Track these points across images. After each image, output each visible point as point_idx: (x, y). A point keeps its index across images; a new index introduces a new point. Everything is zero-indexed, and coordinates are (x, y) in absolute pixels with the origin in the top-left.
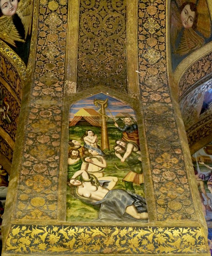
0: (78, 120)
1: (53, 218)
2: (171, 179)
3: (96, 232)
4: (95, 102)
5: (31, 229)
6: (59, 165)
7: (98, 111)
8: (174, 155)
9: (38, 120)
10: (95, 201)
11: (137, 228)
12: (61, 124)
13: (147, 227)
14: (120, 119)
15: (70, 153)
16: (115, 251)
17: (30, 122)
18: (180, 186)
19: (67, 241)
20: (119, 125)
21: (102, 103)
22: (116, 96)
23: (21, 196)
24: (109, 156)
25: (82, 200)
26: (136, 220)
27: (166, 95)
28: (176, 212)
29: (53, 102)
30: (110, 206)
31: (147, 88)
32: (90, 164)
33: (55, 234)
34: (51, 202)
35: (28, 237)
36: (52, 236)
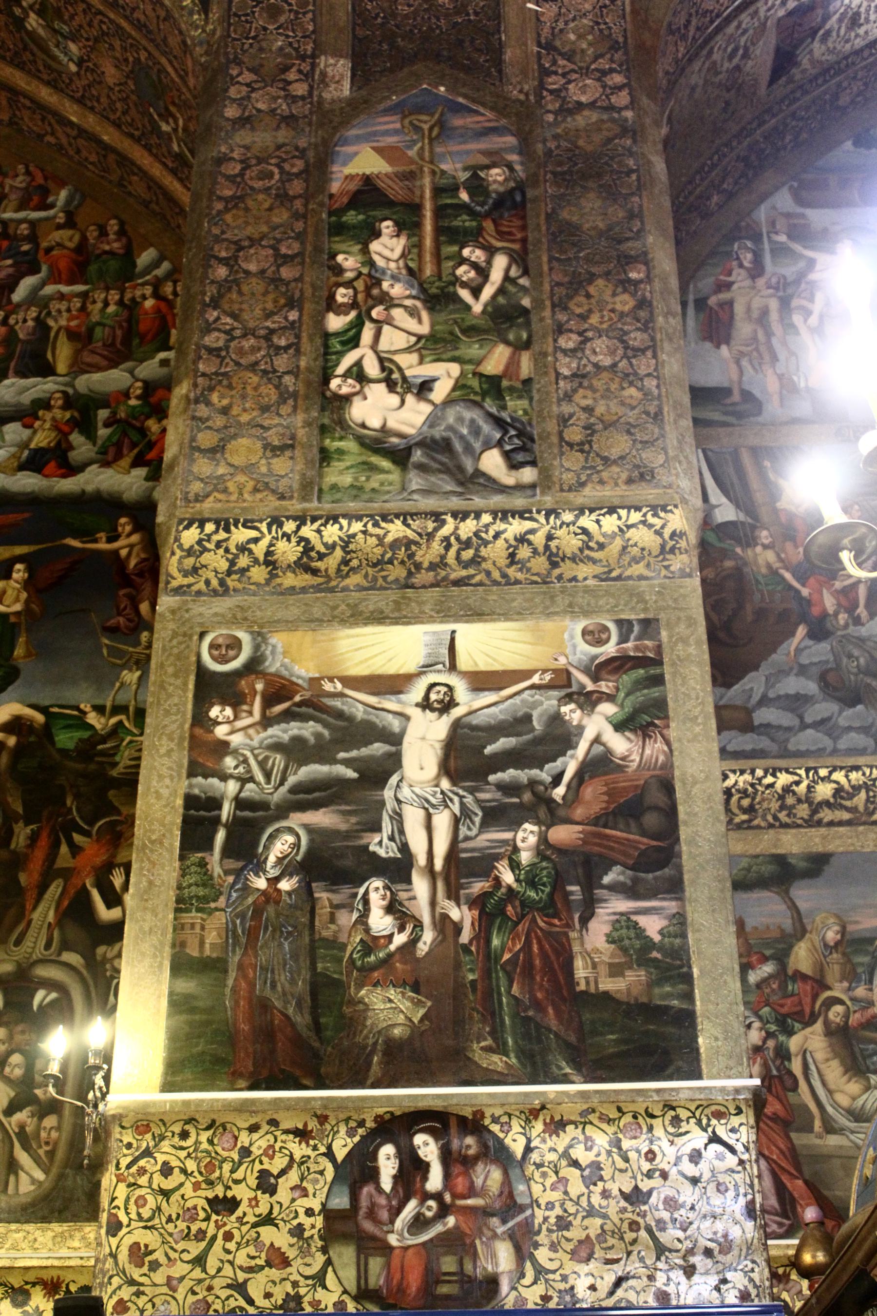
0: (353, 187)
1: (282, 497)
2: (607, 361)
3: (396, 530)
4: (407, 121)
5: (227, 530)
6: (298, 337)
7: (412, 153)
8: (627, 285)
9: (242, 198)
10: (395, 440)
11: (504, 515)
12: (305, 206)
13: (531, 512)
14: (475, 176)
15: (332, 297)
16: (445, 579)
17: (219, 206)
18: (631, 384)
19: (321, 557)
20: (471, 195)
21: (426, 122)
22: (465, 96)
23: (200, 436)
24: (438, 297)
25: (361, 441)
26: (503, 489)
27: (618, 79)
28: (615, 462)
29: (283, 135)
30: (436, 453)
31: (561, 62)
32: (386, 328)
33: (289, 540)
34: (276, 450)
35: (221, 551)
36: (282, 546)
